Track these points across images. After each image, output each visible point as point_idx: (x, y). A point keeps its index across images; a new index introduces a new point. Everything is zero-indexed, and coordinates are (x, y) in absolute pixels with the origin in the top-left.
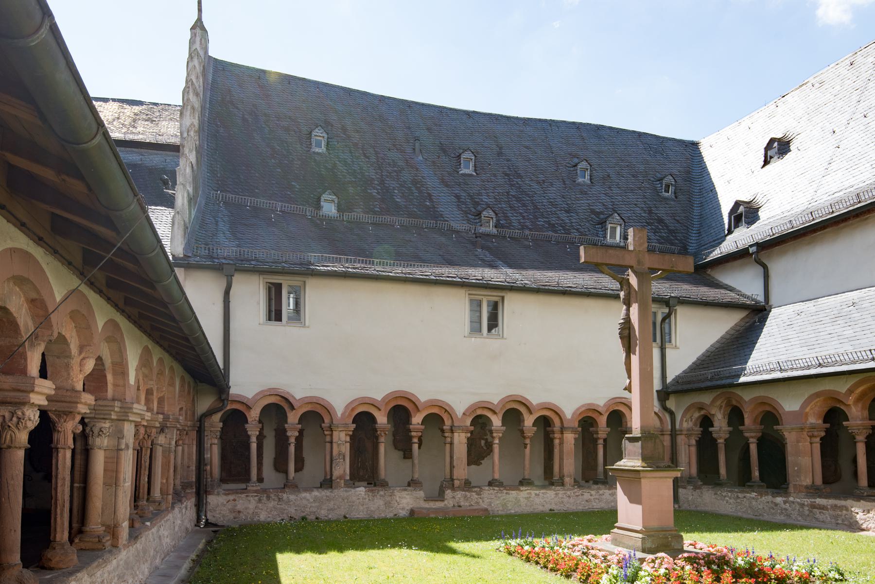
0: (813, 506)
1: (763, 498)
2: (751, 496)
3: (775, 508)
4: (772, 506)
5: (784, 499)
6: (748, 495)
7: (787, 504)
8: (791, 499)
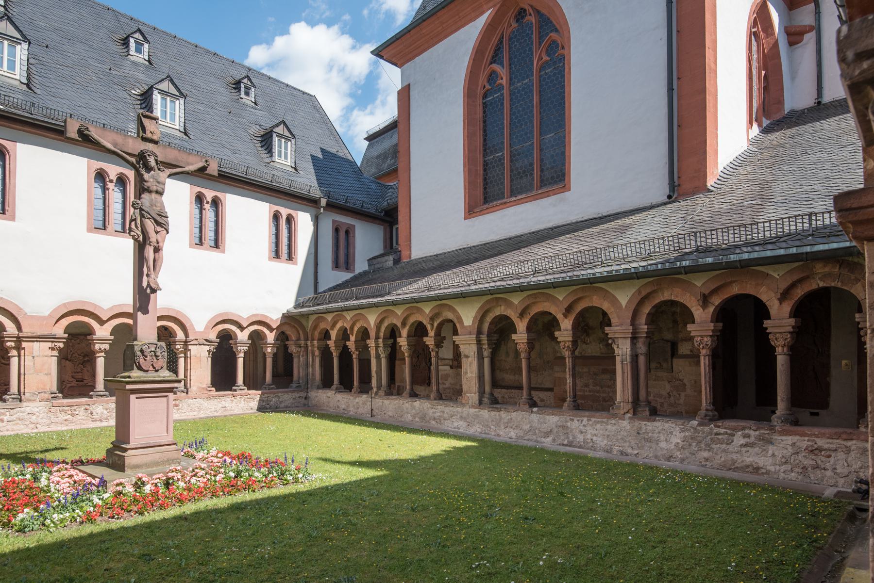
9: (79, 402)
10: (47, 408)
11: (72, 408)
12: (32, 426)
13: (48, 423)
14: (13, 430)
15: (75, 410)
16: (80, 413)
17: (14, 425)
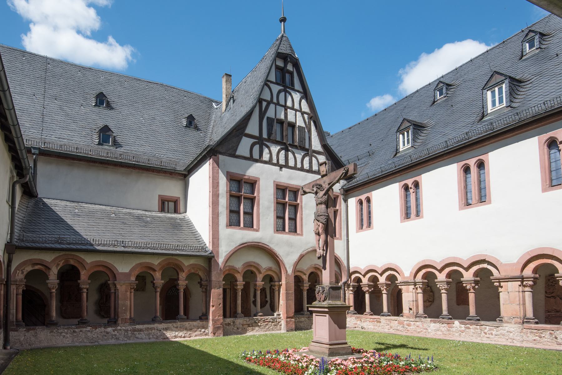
0: (134, 330)
1: (97, 330)
2: (87, 329)
3: (107, 335)
4: (105, 334)
5: (113, 328)
6: (84, 329)
7: (116, 332)
8: (119, 328)
9: (544, 327)
10: (520, 329)
11: (539, 332)
12: (510, 340)
13: (521, 340)
14: (498, 341)
15: (541, 333)
16: (546, 337)
17: (499, 338)
